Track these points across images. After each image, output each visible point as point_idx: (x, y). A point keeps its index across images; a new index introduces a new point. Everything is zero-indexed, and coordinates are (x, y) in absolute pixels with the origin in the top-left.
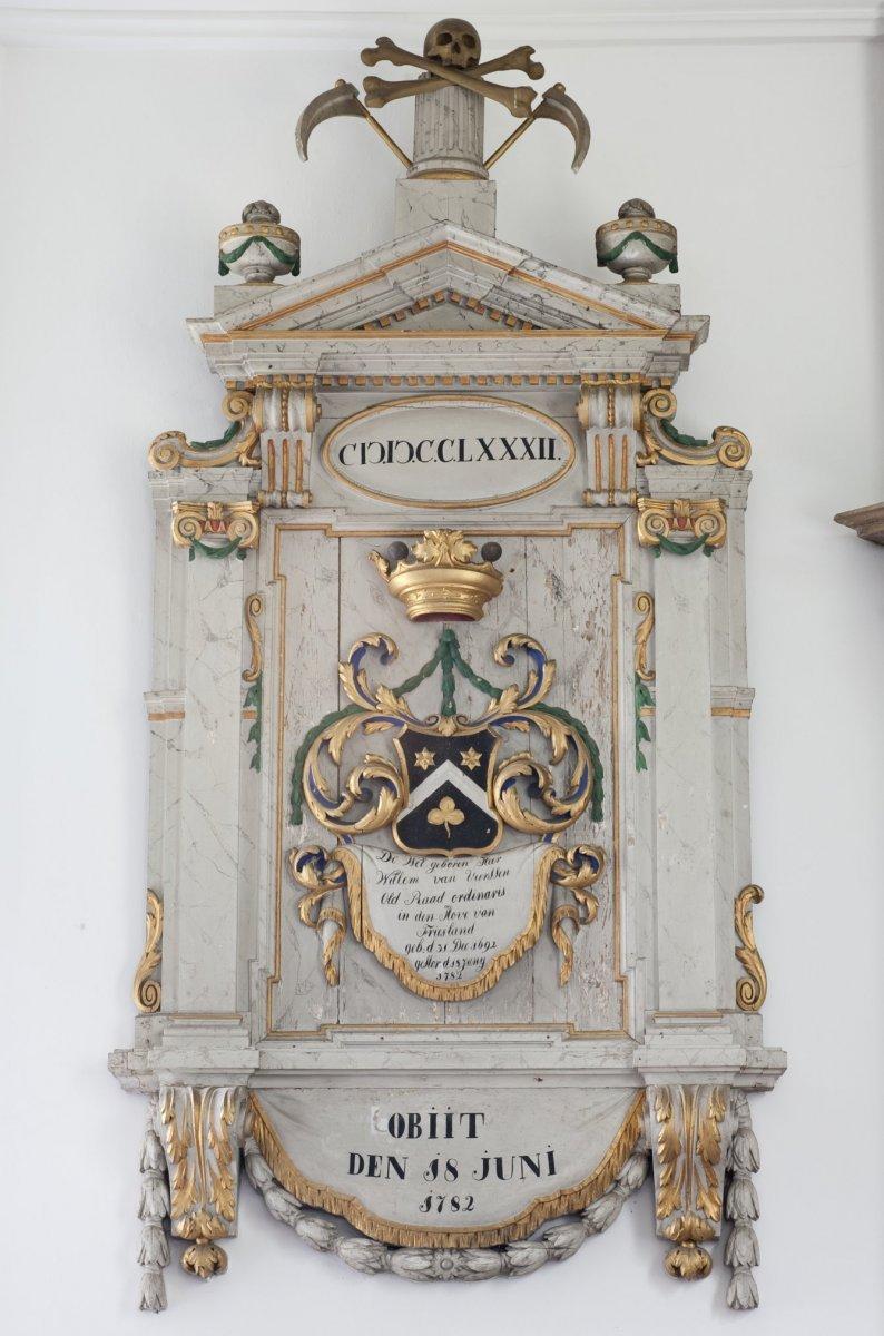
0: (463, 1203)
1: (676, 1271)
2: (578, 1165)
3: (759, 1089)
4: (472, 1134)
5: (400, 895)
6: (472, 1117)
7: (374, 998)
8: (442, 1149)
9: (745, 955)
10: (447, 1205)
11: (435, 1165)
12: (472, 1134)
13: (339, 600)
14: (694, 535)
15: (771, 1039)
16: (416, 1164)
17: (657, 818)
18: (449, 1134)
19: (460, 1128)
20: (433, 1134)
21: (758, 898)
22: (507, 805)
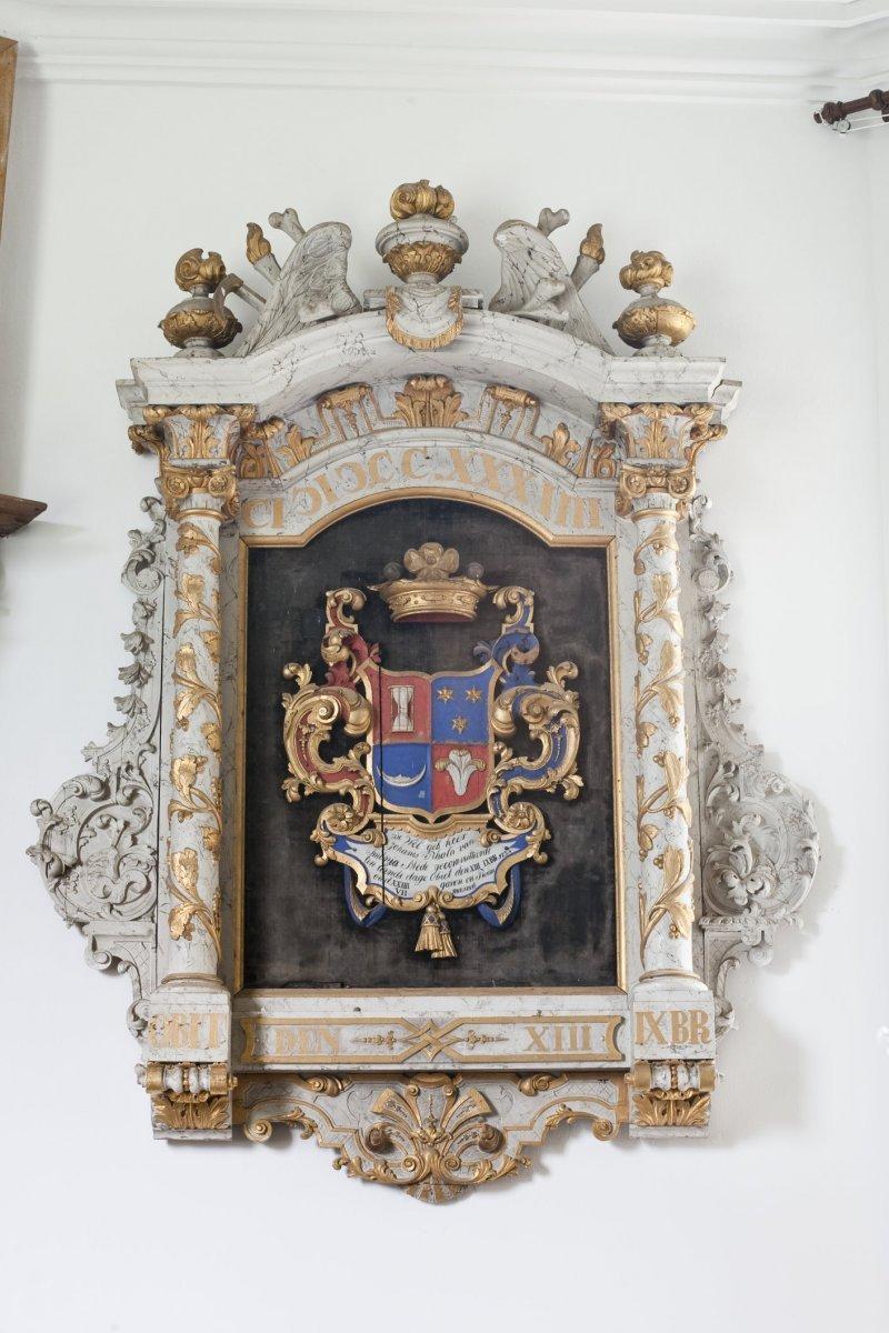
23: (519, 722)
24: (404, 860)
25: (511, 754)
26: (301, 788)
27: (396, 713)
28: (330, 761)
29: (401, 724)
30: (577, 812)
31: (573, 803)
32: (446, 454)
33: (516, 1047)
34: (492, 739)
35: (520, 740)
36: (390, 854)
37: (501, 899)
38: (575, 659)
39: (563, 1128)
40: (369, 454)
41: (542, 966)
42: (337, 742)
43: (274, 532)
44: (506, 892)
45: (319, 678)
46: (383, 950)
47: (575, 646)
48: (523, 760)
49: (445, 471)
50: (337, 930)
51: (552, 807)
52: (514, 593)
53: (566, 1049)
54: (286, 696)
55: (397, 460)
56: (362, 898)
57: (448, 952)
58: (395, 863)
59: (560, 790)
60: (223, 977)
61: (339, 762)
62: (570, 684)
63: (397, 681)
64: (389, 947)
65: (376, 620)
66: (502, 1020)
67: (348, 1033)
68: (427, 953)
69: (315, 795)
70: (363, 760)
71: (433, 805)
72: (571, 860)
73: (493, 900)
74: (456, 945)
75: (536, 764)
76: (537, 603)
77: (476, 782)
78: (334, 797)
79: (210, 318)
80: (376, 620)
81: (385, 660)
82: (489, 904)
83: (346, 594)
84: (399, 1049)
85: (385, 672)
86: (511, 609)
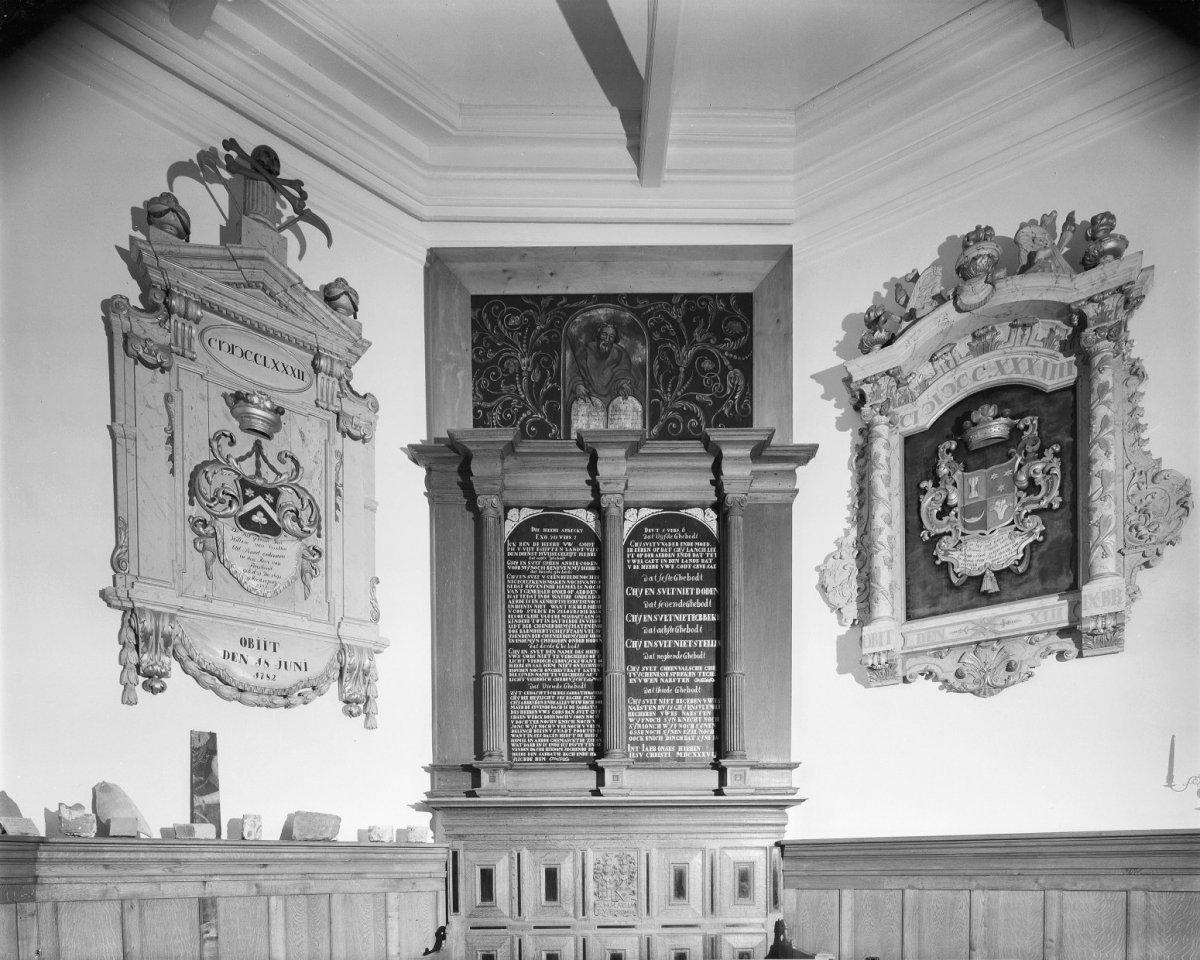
0: (272, 677)
1: (351, 714)
2: (317, 667)
3: (377, 652)
4: (275, 651)
6: (275, 644)
8: (261, 654)
9: (374, 603)
10: (265, 676)
11: (260, 661)
12: (275, 651)
15: (382, 634)
16: (252, 660)
18: (265, 649)
19: (270, 647)
20: (259, 648)
21: (378, 582)
23: (1031, 480)
24: (975, 554)
25: (1025, 494)
26: (929, 535)
27: (976, 487)
28: (941, 519)
29: (974, 494)
30: (1058, 515)
31: (1057, 510)
32: (994, 365)
34: (1016, 490)
35: (1032, 488)
36: (968, 553)
37: (1020, 561)
38: (1058, 442)
40: (957, 376)
41: (1039, 588)
42: (946, 509)
43: (914, 426)
44: (1023, 558)
45: (936, 485)
46: (965, 595)
47: (1059, 437)
48: (1032, 496)
49: (993, 373)
50: (946, 590)
51: (1047, 516)
52: (1028, 420)
53: (1049, 620)
54: (922, 496)
55: (970, 375)
56: (956, 575)
57: (997, 589)
58: (970, 556)
59: (1051, 505)
61: (945, 519)
62: (1056, 455)
63: (970, 477)
67: (948, 630)
68: (986, 592)
69: (936, 536)
70: (956, 515)
72: (1055, 537)
73: (1017, 563)
74: (999, 586)
75: (1040, 496)
76: (1040, 422)
77: (1010, 510)
78: (945, 534)
81: (966, 469)
82: (1015, 565)
83: (947, 444)
84: (970, 633)
85: (966, 474)
86: (1027, 428)
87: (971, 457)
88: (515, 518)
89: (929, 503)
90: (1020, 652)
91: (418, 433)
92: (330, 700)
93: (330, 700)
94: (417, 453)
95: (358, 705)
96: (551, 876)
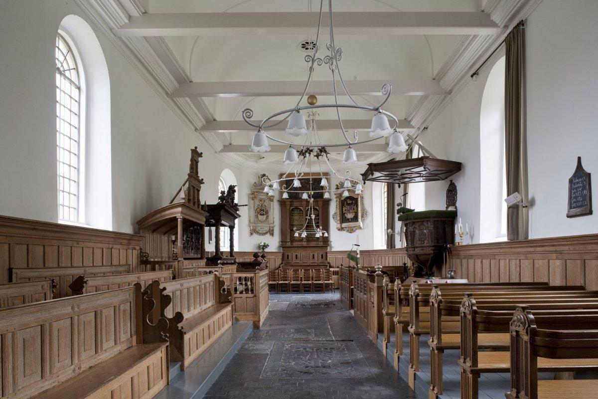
5: (260, 217)
7: (259, 222)
13: (257, 203)
14: (272, 201)
17: (271, 213)
22: (264, 213)
33: (353, 226)
39: (356, 229)
60: (340, 223)
64: (348, 221)
65: (347, 203)
66: (352, 224)
71: (350, 213)
79: (337, 188)
80: (347, 203)
87: (348, 204)
88: (292, 208)
89: (344, 209)
90: (354, 229)
91: (278, 199)
92: (268, 234)
93: (268, 234)
94: (278, 201)
95: (272, 234)
96: (296, 255)
